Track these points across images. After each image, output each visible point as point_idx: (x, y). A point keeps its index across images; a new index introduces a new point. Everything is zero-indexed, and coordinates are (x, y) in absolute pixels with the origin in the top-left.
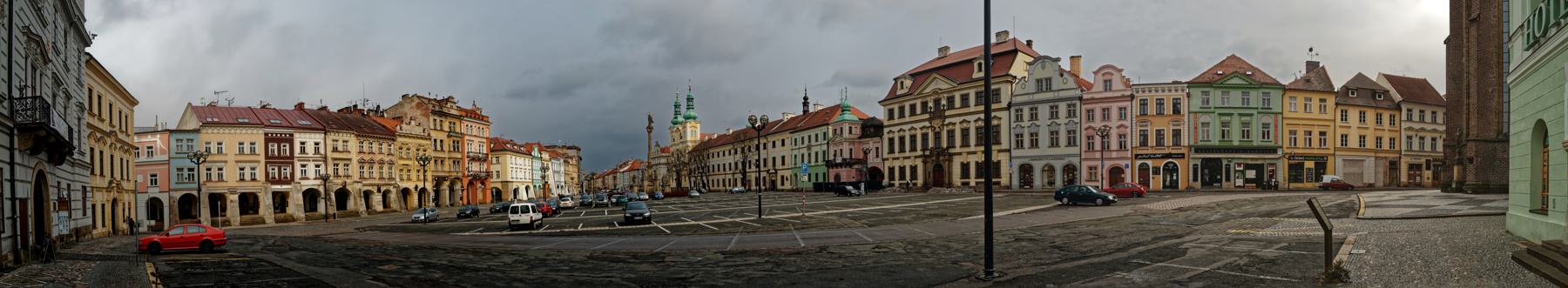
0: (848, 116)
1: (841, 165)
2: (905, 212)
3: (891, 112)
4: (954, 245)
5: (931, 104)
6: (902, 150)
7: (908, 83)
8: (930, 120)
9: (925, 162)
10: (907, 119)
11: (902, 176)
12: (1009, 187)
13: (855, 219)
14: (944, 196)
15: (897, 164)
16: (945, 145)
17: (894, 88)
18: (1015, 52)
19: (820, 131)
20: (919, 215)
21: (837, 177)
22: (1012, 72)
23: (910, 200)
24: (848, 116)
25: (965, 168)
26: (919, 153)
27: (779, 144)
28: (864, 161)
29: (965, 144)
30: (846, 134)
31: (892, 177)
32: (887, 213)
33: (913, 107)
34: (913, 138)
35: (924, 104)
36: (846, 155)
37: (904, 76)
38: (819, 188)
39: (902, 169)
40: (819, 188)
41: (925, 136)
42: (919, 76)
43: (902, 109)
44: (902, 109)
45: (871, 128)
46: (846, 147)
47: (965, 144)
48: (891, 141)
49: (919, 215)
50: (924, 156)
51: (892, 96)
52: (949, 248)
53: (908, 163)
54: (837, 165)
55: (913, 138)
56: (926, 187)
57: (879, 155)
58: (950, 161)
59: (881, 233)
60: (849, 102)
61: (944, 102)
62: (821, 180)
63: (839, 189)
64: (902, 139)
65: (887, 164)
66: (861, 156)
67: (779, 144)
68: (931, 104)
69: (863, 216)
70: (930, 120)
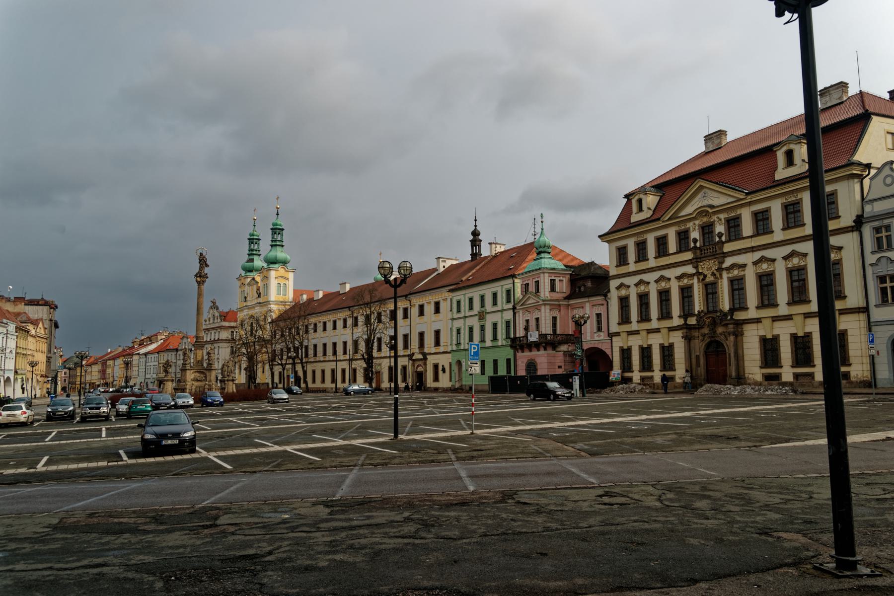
0: (547, 262)
1: (537, 345)
2: (655, 430)
3: (622, 254)
4: (760, 496)
5: (695, 234)
6: (644, 317)
7: (651, 200)
8: (694, 262)
9: (688, 339)
10: (652, 263)
11: (647, 365)
12: (870, 384)
13: (565, 441)
14: (729, 401)
15: (635, 343)
16: (725, 305)
17: (626, 212)
18: (864, 118)
19: (500, 288)
20: (683, 437)
21: (531, 366)
22: (862, 155)
23: (663, 407)
24: (547, 262)
25: (770, 347)
26: (677, 321)
27: (429, 309)
28: (576, 338)
29: (767, 298)
30: (545, 292)
31: (626, 365)
32: (622, 430)
33: (662, 243)
34: (664, 295)
35: (683, 236)
36: (546, 328)
37: (643, 190)
38: (500, 385)
39: (646, 352)
40: (500, 385)
41: (686, 293)
42: (671, 187)
43: (641, 247)
44: (641, 247)
45: (587, 281)
46: (546, 315)
47: (767, 298)
48: (624, 302)
49: (683, 437)
50: (686, 327)
51: (624, 224)
52: (749, 501)
53: (656, 342)
54: (531, 346)
55: (664, 295)
56: (691, 386)
57: (602, 327)
58: (738, 334)
59: (613, 468)
60: (548, 239)
61: (720, 228)
62: (502, 371)
63: (534, 387)
64: (643, 299)
65: (618, 343)
66: (571, 329)
67: (429, 309)
68: (695, 234)
69: (578, 436)
70: (694, 262)
